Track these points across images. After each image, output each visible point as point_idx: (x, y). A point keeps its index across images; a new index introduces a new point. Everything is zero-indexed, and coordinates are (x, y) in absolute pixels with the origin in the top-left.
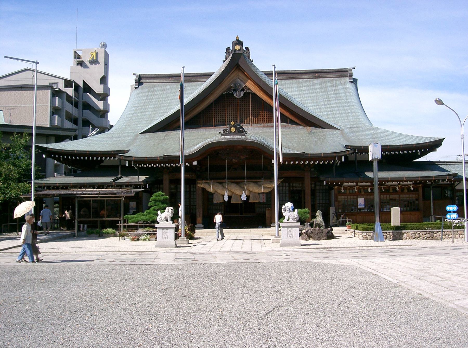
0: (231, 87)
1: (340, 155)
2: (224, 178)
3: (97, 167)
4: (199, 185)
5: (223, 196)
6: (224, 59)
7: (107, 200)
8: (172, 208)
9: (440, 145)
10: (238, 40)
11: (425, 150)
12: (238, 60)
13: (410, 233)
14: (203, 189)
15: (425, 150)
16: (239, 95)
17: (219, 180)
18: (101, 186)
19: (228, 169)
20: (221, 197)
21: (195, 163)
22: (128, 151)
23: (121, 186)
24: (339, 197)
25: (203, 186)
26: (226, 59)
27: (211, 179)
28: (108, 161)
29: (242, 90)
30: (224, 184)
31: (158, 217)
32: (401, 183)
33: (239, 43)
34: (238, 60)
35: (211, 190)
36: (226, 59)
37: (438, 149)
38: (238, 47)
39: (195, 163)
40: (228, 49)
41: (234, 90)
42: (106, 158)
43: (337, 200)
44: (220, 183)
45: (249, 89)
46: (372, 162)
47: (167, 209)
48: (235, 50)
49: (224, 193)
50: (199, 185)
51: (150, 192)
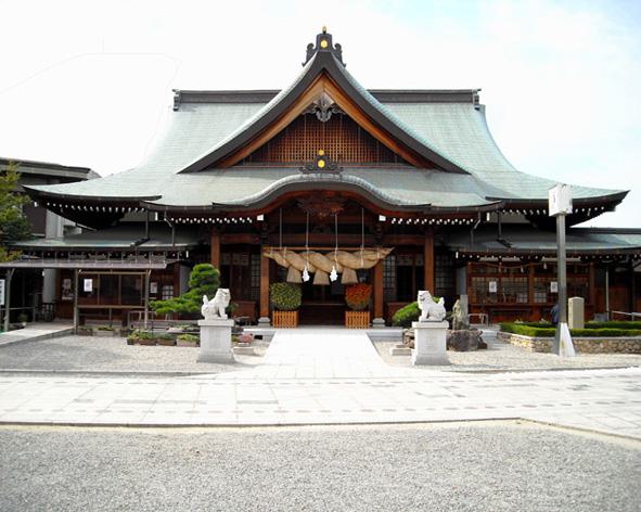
0: (313, 104)
1: (484, 209)
2: (303, 245)
3: (114, 224)
4: (266, 255)
5: (302, 273)
6: (304, 61)
7: (123, 276)
8: (227, 290)
9: (620, 201)
10: (324, 32)
11: (599, 208)
12: (325, 62)
13: (610, 342)
14: (272, 261)
15: (599, 208)
16: (324, 117)
17: (297, 247)
18: (116, 254)
19: (310, 231)
20: (298, 274)
21: (260, 218)
22: (160, 197)
23: (146, 253)
24: (474, 279)
25: (270, 256)
26: (308, 60)
27: (283, 246)
28: (131, 216)
29: (330, 109)
30: (304, 253)
31: (204, 307)
32: (504, 259)
33: (325, 36)
34: (325, 62)
35: (284, 263)
36: (308, 60)
37: (618, 207)
38: (324, 44)
39: (260, 218)
40: (310, 46)
41: (318, 109)
42: (133, 209)
43: (469, 283)
44: (298, 252)
45: (339, 108)
46: (554, 218)
47: (218, 292)
48: (321, 48)
49: (303, 265)
50: (266, 255)
51: (190, 265)
